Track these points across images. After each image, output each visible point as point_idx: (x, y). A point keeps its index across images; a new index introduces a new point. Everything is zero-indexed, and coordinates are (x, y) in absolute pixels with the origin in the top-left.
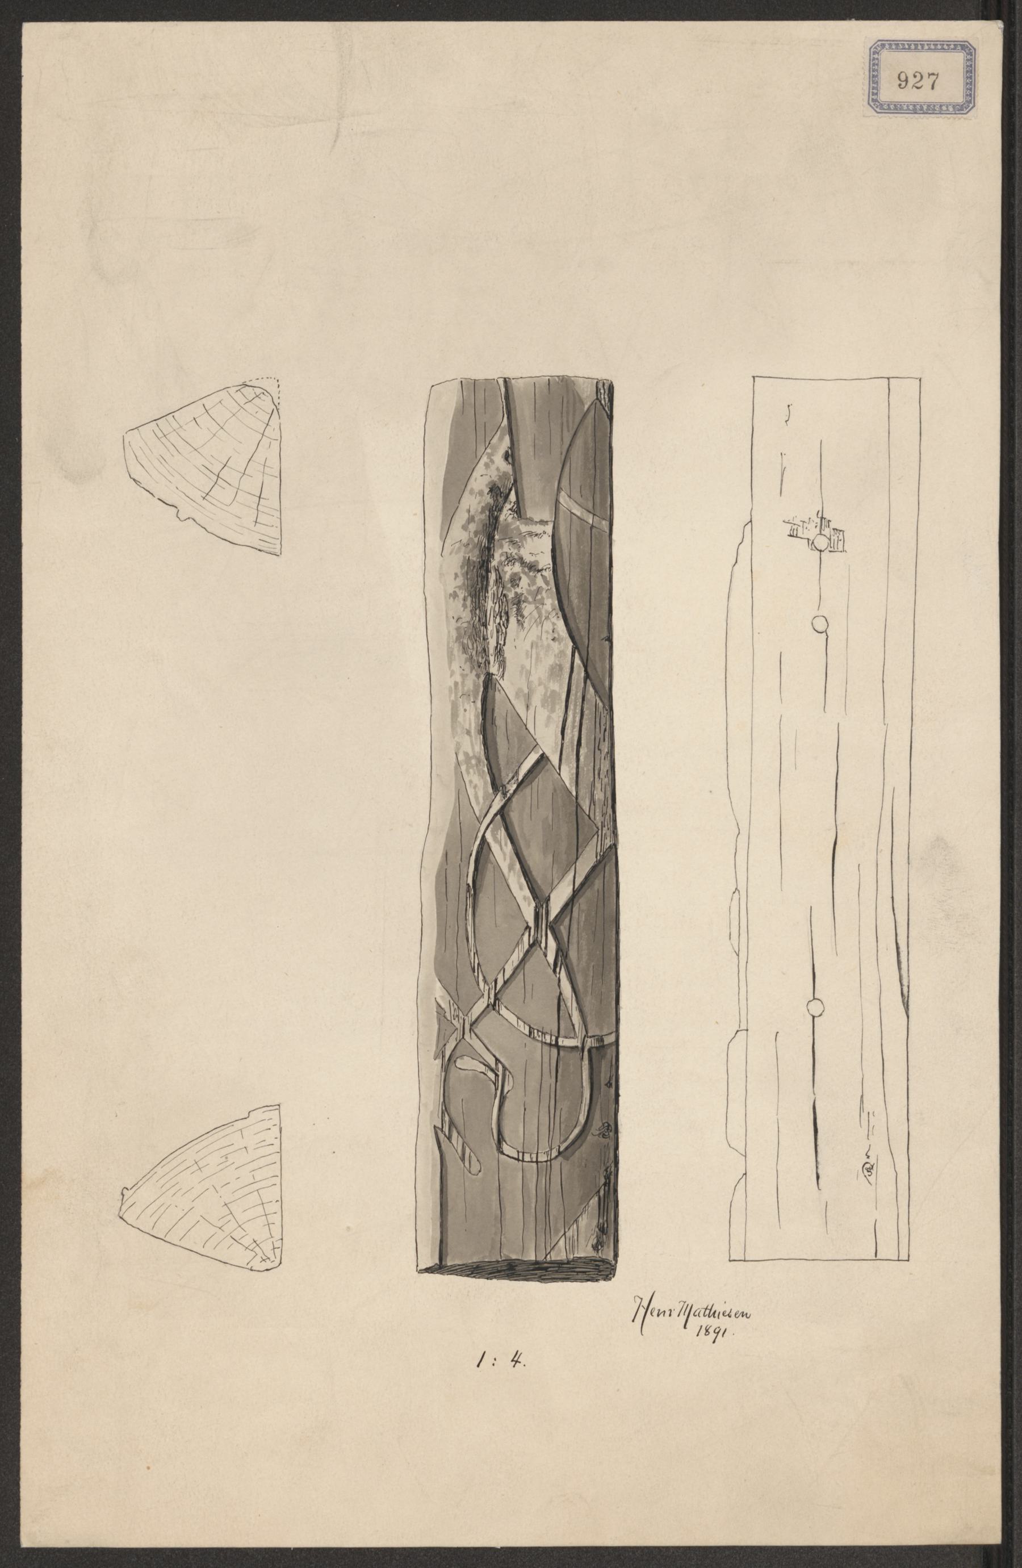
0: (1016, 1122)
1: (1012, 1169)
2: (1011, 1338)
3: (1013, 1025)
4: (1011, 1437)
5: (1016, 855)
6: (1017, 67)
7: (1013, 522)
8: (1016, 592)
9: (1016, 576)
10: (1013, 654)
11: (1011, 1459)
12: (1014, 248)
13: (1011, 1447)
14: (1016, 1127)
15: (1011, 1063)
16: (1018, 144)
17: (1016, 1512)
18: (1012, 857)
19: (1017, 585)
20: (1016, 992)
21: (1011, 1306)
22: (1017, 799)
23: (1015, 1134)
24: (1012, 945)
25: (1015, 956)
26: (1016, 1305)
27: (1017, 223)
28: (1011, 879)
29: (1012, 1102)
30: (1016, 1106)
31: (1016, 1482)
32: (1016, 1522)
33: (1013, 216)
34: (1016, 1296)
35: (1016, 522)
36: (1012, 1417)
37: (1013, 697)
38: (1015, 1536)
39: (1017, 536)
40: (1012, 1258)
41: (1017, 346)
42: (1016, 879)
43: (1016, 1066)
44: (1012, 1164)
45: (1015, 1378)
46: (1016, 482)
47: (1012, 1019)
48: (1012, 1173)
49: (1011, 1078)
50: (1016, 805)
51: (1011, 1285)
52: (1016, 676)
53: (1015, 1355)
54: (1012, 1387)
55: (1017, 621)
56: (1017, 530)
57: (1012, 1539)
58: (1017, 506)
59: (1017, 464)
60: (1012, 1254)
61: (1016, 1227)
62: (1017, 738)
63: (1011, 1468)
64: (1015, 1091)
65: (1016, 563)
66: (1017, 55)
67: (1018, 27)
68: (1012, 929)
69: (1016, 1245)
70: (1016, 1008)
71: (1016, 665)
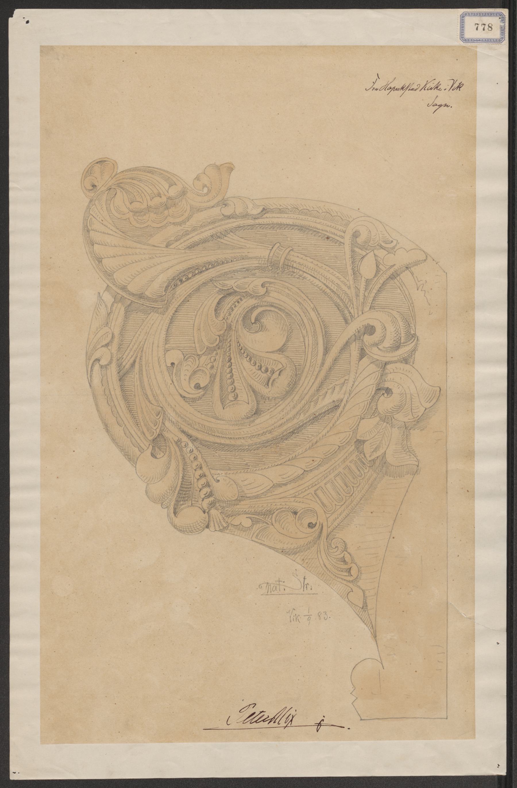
0: (514, 541)
1: (513, 561)
2: (512, 632)
3: (513, 500)
4: (512, 675)
5: (515, 428)
7: (514, 287)
8: (515, 317)
9: (515, 310)
10: (514, 342)
12: (514, 171)
13: (512, 679)
14: (514, 543)
17: (514, 707)
18: (513, 429)
19: (515, 314)
20: (515, 486)
21: (512, 619)
22: (515, 405)
23: (514, 546)
24: (513, 466)
25: (514, 471)
32: (514, 711)
33: (514, 157)
34: (514, 615)
35: (515, 287)
36: (512, 666)
37: (514, 361)
38: (514, 716)
40: (513, 599)
44: (513, 559)
45: (514, 649)
46: (515, 270)
47: (513, 497)
48: (513, 563)
49: (512, 522)
50: (515, 407)
52: (515, 352)
53: (514, 639)
54: (512, 653)
55: (515, 329)
56: (516, 290)
57: (512, 717)
59: (516, 262)
60: (513, 598)
62: (515, 378)
63: (512, 688)
64: (514, 528)
65: (515, 304)
68: (513, 460)
69: (514, 593)
70: (515, 493)
71: (515, 347)
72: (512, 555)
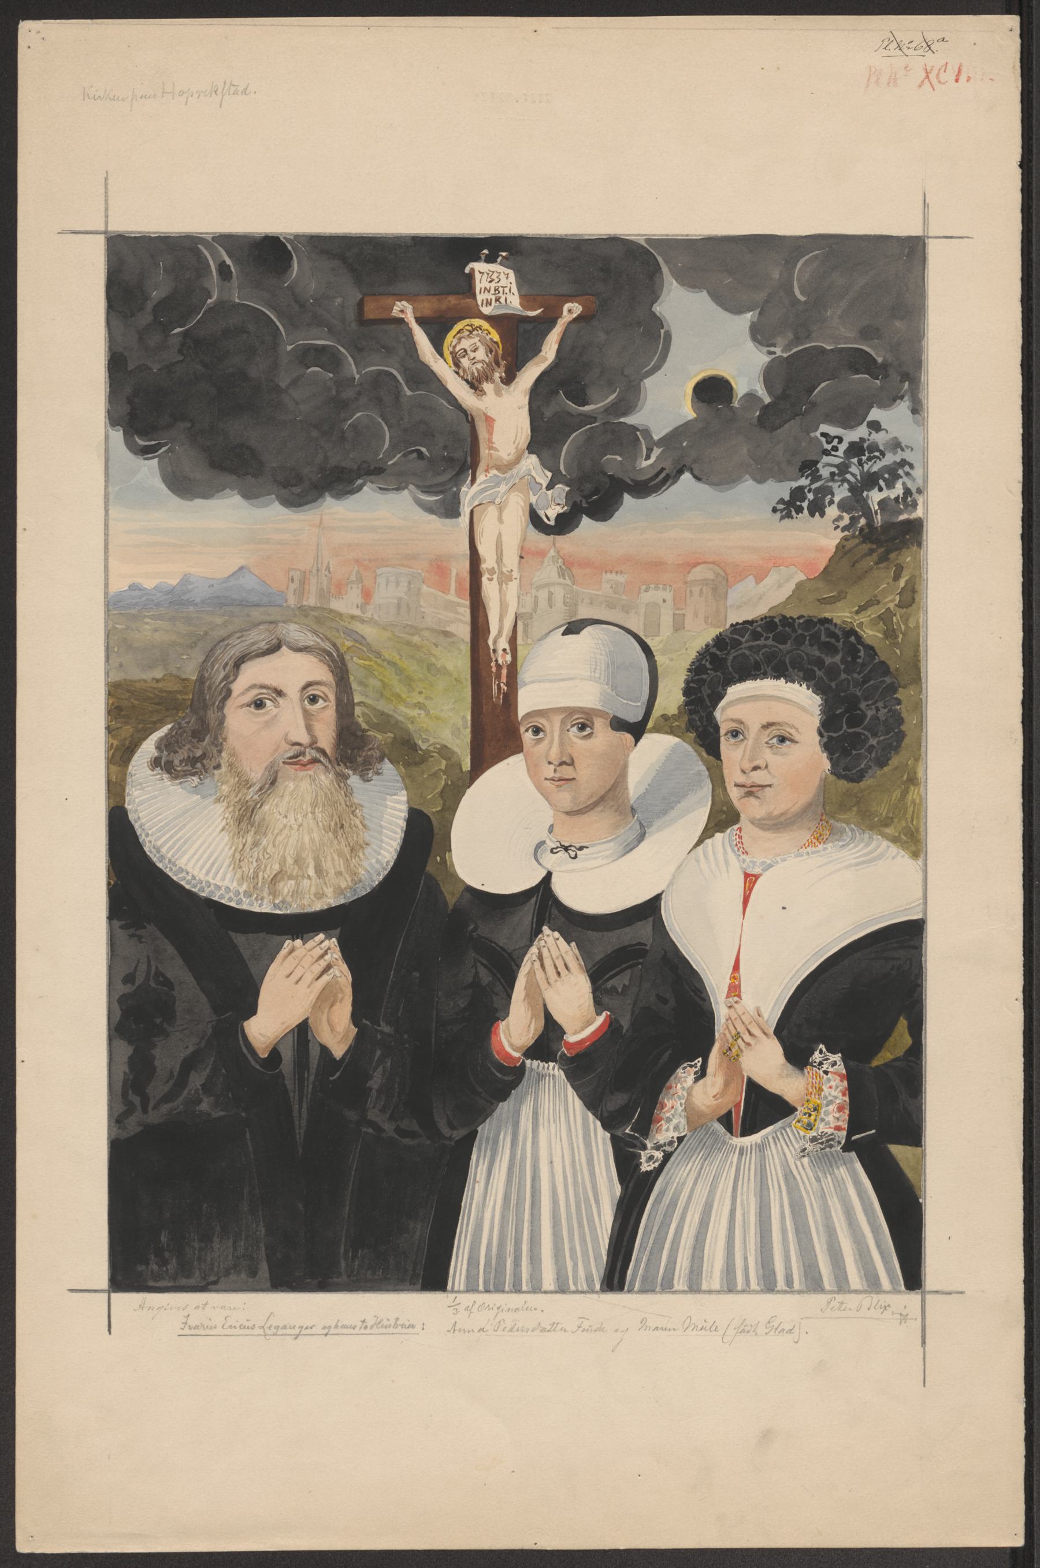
5: (1035, 921)
6: (1034, 330)
8: (1034, 723)
11: (1032, 1373)
13: (1032, 1364)
15: (1032, 1077)
16: (1035, 388)
19: (1035, 718)
21: (1032, 1259)
26: (1035, 1257)
27: (1034, 447)
28: (1031, 938)
29: (1032, 1106)
30: (1035, 1109)
31: (1036, 1390)
34: (1036, 1251)
39: (1035, 682)
41: (1035, 541)
42: (1035, 938)
43: (1035, 1079)
45: (1035, 1313)
51: (1032, 1242)
53: (1035, 1294)
54: (1032, 1319)
55: (1035, 746)
58: (1035, 659)
59: (1035, 627)
61: (1035, 1199)
63: (1032, 1380)
66: (1034, 321)
67: (1034, 300)
70: (1035, 1036)
72: (1031, 1145)
